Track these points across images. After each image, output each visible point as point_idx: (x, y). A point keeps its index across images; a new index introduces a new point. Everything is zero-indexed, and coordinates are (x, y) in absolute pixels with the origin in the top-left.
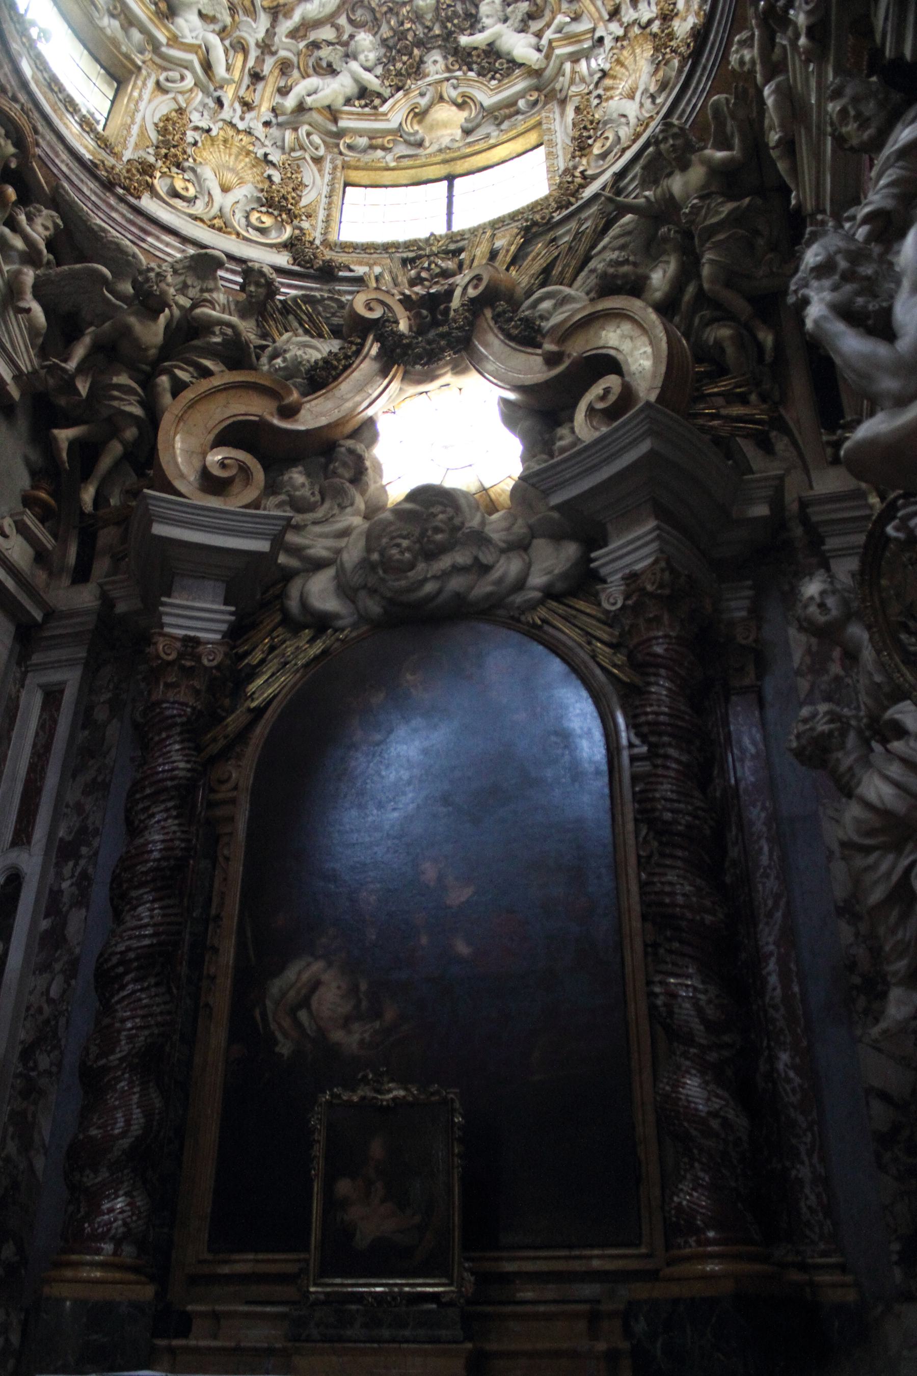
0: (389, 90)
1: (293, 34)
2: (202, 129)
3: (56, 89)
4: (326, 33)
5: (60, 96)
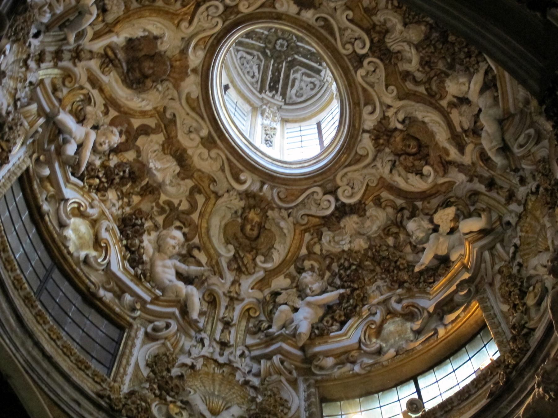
0: (481, 64)
1: (461, 149)
2: (514, 253)
3: (450, 407)
4: (455, 115)
5: (455, 404)
